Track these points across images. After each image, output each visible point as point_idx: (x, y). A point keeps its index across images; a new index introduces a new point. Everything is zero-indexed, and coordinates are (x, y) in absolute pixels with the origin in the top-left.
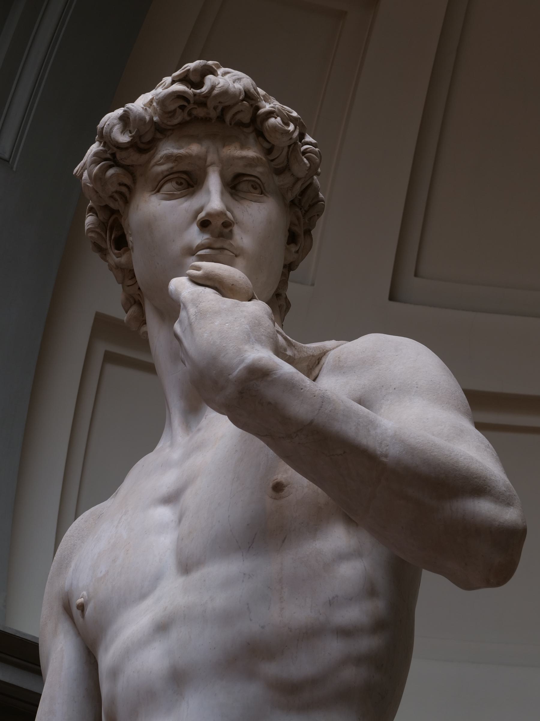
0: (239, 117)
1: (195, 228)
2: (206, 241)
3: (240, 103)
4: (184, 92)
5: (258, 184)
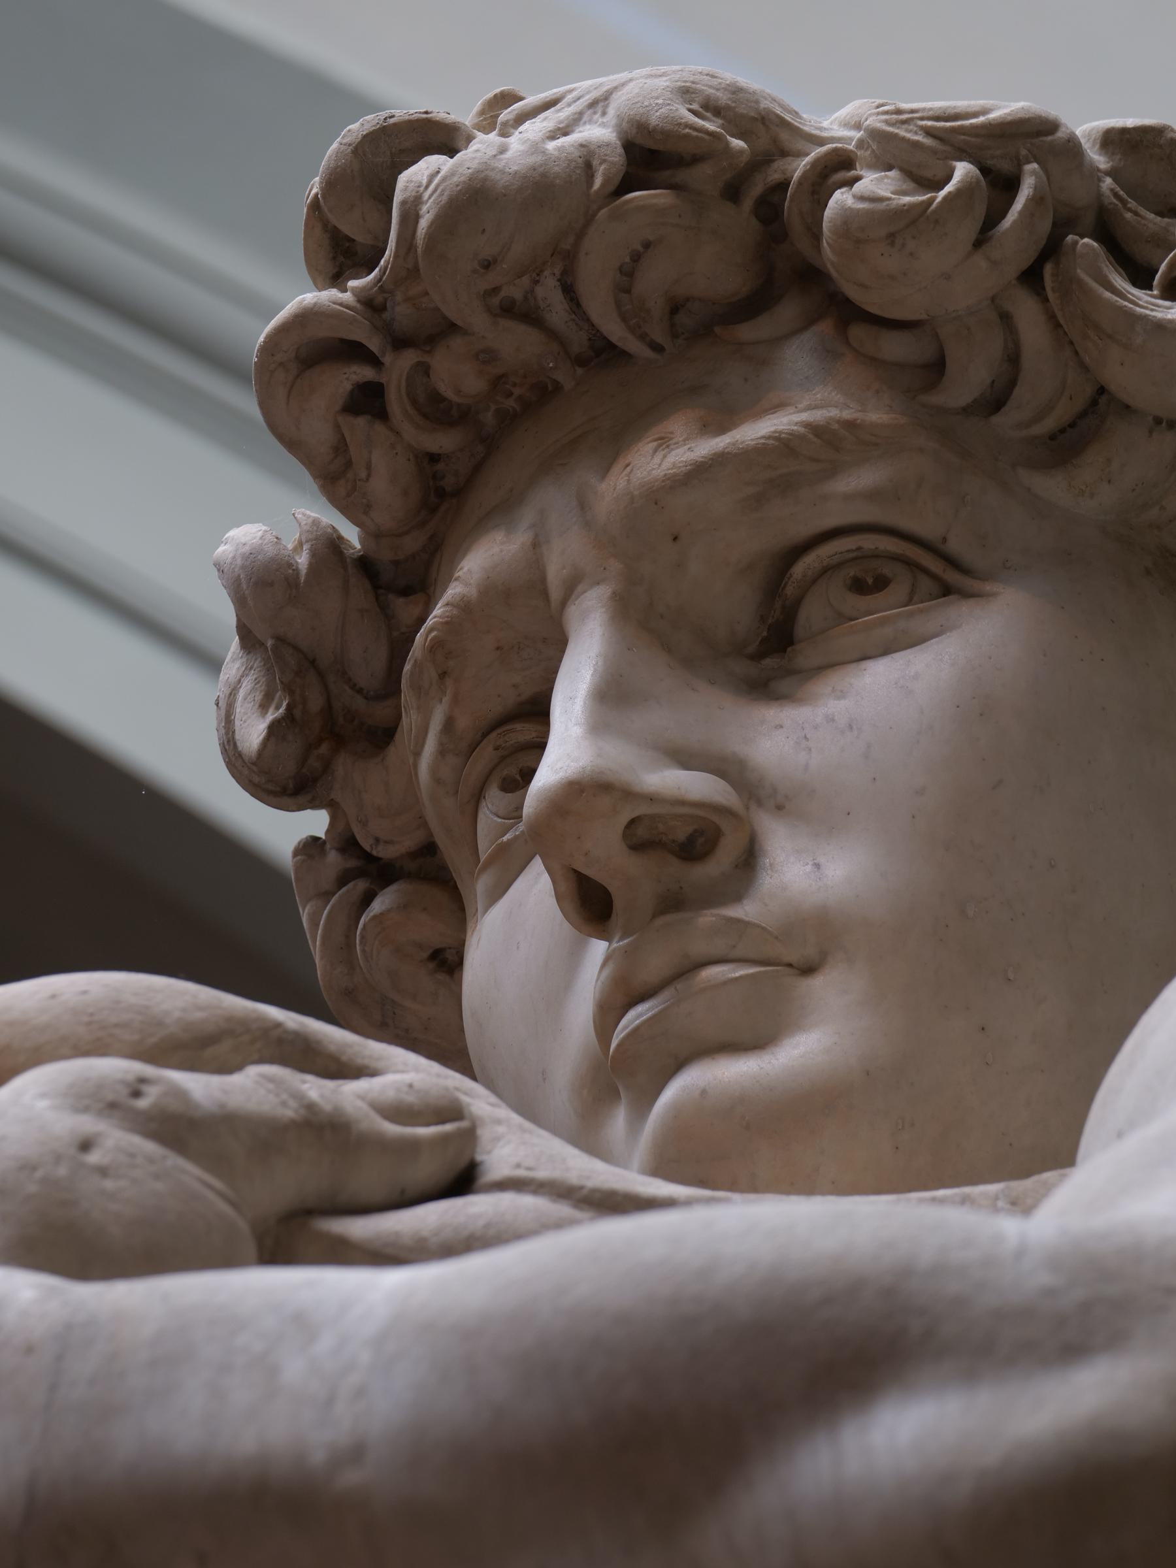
0: (655, 280)
1: (598, 949)
2: (607, 972)
3: (604, 212)
4: (304, 318)
5: (876, 555)
